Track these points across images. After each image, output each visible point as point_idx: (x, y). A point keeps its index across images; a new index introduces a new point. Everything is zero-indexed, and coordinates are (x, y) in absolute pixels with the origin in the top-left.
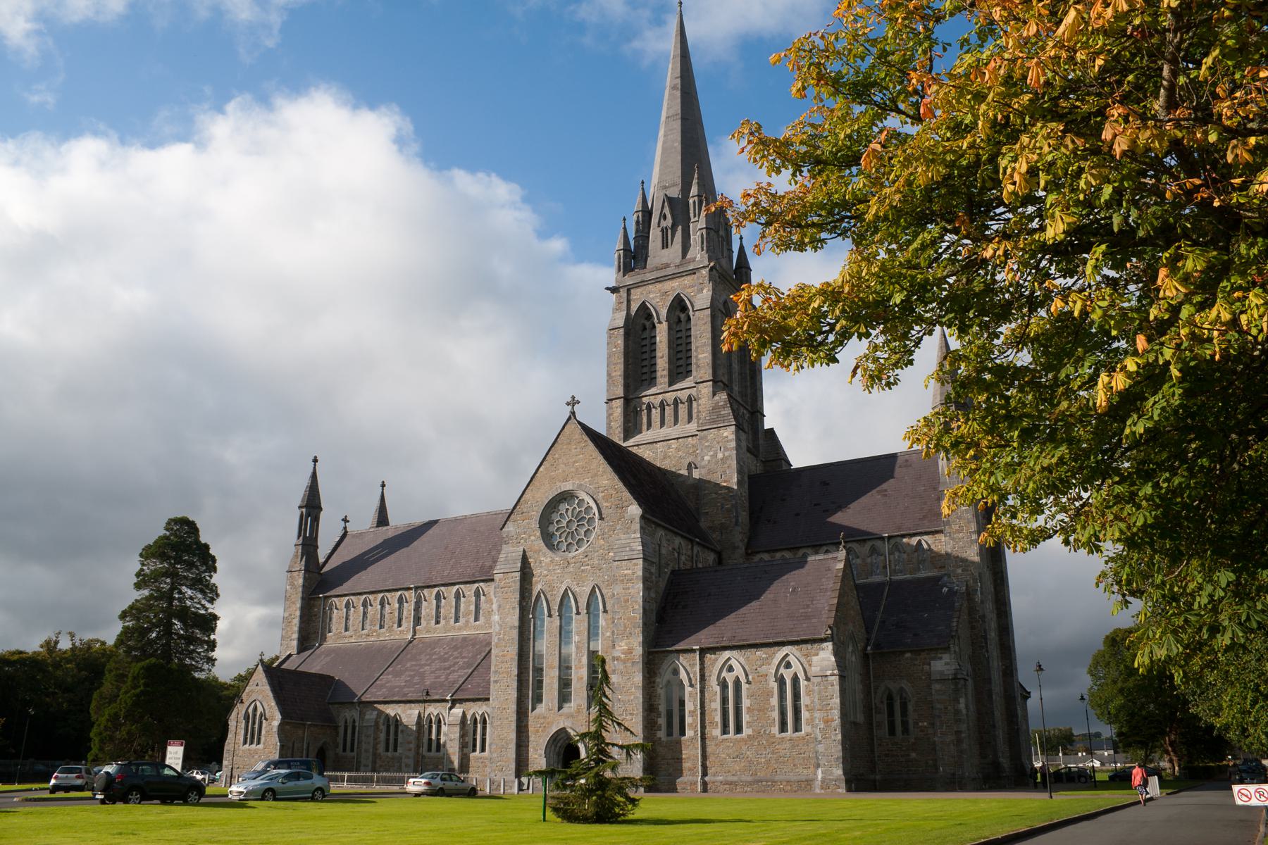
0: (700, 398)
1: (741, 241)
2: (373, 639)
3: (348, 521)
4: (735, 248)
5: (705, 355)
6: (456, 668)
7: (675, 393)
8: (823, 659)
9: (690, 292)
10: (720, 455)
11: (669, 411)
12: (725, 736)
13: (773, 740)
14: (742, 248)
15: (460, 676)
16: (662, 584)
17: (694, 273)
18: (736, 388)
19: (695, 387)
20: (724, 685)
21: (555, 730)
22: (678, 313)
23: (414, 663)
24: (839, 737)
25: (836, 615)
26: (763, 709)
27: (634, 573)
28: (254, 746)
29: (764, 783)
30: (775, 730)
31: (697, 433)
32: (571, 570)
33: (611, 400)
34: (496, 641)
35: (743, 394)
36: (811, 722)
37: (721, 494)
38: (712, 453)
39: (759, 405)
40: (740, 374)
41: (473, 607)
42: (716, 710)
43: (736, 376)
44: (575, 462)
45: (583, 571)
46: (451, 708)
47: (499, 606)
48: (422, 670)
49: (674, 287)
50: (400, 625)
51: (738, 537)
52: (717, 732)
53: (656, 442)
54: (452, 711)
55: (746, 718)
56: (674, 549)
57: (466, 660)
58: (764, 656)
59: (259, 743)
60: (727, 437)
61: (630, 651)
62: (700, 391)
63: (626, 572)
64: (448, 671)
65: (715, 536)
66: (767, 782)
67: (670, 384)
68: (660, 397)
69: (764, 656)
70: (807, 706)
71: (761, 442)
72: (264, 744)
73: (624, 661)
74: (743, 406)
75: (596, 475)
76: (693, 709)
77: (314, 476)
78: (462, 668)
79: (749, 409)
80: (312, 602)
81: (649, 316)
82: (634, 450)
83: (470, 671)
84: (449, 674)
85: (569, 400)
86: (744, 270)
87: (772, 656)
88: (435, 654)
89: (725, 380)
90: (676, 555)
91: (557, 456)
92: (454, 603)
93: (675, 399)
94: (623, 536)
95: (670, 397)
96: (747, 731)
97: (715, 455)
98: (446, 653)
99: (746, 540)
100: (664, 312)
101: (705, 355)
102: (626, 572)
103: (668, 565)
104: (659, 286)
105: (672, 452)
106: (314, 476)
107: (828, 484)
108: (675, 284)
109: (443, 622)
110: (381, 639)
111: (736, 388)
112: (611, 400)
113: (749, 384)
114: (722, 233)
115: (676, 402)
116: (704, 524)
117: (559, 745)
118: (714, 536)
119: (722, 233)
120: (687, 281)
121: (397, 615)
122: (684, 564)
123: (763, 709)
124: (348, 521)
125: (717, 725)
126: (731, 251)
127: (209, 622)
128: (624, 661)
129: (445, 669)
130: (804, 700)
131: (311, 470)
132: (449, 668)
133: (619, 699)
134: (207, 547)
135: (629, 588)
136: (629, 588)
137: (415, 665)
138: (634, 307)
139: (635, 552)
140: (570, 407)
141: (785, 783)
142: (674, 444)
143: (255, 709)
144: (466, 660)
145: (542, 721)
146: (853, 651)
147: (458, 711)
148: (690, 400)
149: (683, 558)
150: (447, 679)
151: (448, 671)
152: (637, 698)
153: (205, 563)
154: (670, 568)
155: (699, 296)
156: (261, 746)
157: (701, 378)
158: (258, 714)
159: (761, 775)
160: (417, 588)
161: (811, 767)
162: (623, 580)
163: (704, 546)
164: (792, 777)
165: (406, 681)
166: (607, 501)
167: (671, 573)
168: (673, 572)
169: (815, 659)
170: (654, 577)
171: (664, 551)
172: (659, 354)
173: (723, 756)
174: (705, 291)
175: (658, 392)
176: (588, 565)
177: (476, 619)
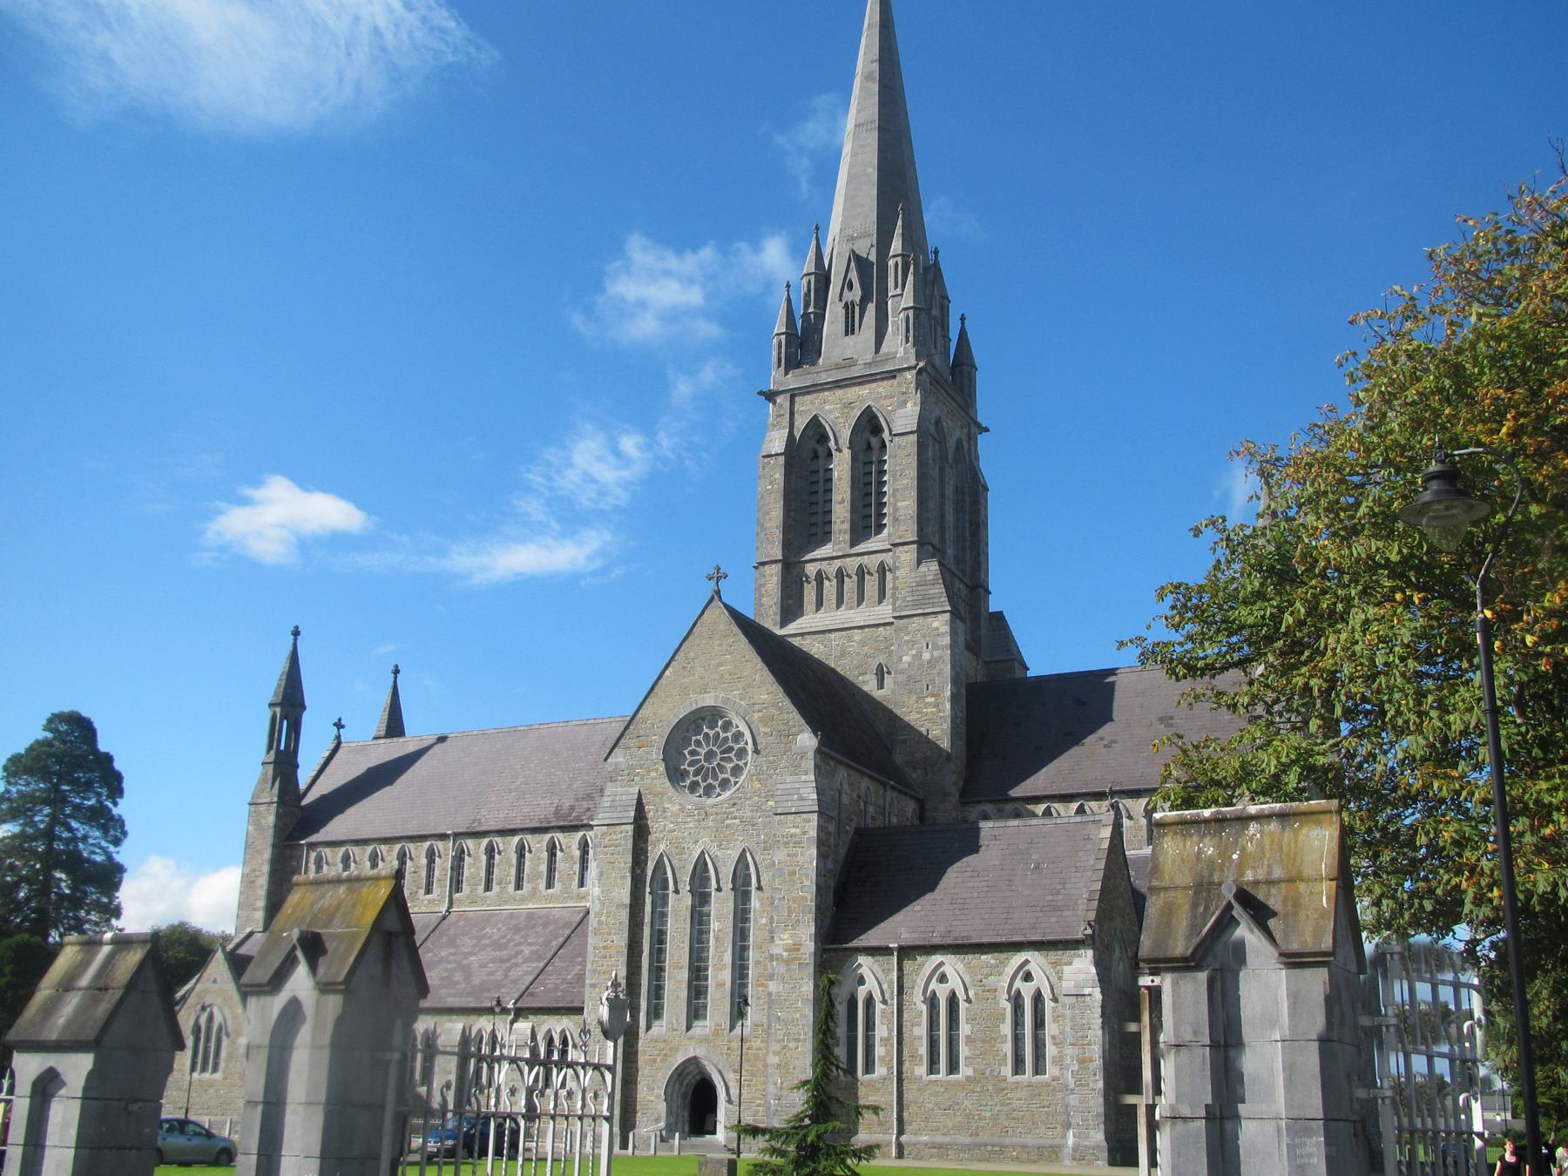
0: (898, 568)
1: (963, 323)
3: (343, 727)
4: (954, 335)
5: (906, 503)
6: (520, 959)
8: (1080, 971)
9: (882, 408)
10: (926, 656)
11: (850, 585)
12: (933, 1077)
13: (1003, 1085)
14: (963, 334)
15: (527, 973)
16: (843, 850)
17: (894, 377)
18: (950, 552)
19: (890, 550)
20: (932, 1002)
21: (680, 1059)
22: (867, 434)
23: (452, 950)
24: (1100, 1084)
25: (1099, 906)
26: (986, 1039)
27: (804, 833)
28: (207, 1075)
29: (989, 1148)
30: (1007, 1070)
31: (893, 620)
32: (711, 824)
33: (763, 564)
34: (595, 925)
35: (959, 560)
36: (1059, 1061)
37: (927, 714)
38: (914, 652)
39: (982, 576)
40: (956, 529)
41: (544, 868)
42: (920, 1038)
43: (950, 534)
44: (720, 665)
45: (728, 826)
46: (512, 1023)
47: (601, 874)
48: (464, 962)
49: (863, 395)
50: (428, 891)
51: (951, 780)
52: (921, 1070)
53: (830, 631)
54: (515, 1025)
55: (964, 1051)
56: (859, 796)
57: (535, 948)
58: (993, 961)
59: (215, 1069)
60: (937, 629)
61: (795, 948)
62: (898, 557)
63: (793, 831)
64: (508, 965)
65: (915, 776)
66: (993, 1146)
67: (854, 542)
68: (838, 563)
69: (993, 961)
70: (1053, 1037)
71: (983, 632)
73: (788, 962)
74: (961, 580)
75: (749, 686)
76: (886, 1035)
78: (527, 960)
79: (966, 581)
80: (288, 851)
81: (824, 438)
82: (796, 642)
83: (542, 965)
84: (508, 970)
85: (712, 571)
86: (966, 369)
87: (1003, 964)
88: (484, 936)
89: (935, 540)
90: (862, 804)
92: (514, 861)
93: (860, 567)
94: (789, 779)
95: (852, 564)
96: (965, 1071)
97: (919, 655)
98: (503, 937)
99: (961, 783)
100: (845, 434)
101: (906, 503)
103: (851, 821)
104: (839, 393)
105: (853, 647)
107: (1084, 704)
108: (864, 391)
109: (496, 888)
111: (950, 552)
112: (763, 564)
113: (968, 544)
114: (935, 312)
115: (861, 572)
116: (899, 757)
117: (686, 1082)
118: (915, 776)
119: (935, 312)
120: (882, 388)
121: (424, 875)
122: (873, 818)
123: (986, 1039)
124: (343, 727)
125: (921, 1059)
126: (947, 338)
127: (110, 876)
128: (788, 962)
129: (502, 961)
130: (1050, 1029)
131: (290, 648)
132: (508, 960)
133: (779, 1018)
134: (108, 759)
135: (796, 855)
136: (796, 855)
137: (455, 954)
138: (801, 423)
139: (806, 803)
140: (713, 583)
141: (1019, 1149)
142: (857, 635)
143: (211, 1018)
144: (535, 948)
145: (662, 1045)
146: (1121, 959)
147: (524, 1026)
148: (882, 570)
149: (871, 809)
150: (506, 976)
151: (508, 965)
152: (804, 1016)
153: (108, 784)
154: (854, 825)
155: (901, 412)
156: (218, 1076)
157: (900, 537)
159: (984, 1137)
160: (457, 835)
161: (1059, 1126)
162: (788, 843)
163: (900, 791)
164: (1030, 1140)
165: (442, 979)
166: (765, 726)
167: (855, 833)
168: (857, 830)
169: (1067, 969)
170: (832, 840)
171: (845, 800)
172: (836, 497)
173: (930, 1106)
174: (909, 405)
175: (834, 554)
177: (549, 885)
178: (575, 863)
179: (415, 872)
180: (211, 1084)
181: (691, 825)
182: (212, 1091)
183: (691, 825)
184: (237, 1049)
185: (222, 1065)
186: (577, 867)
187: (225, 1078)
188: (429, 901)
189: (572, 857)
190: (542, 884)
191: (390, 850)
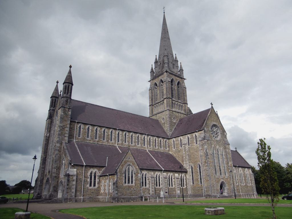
2: (100, 143)
41: (137, 141)
72: (135, 183)
77: (70, 72)
92: (131, 138)
106: (70, 72)
110: (104, 144)
121: (110, 136)
143: (129, 169)
179: (108, 136)
180: (132, 187)
182: (132, 189)
184: (138, 177)
186: (143, 142)
187: (136, 185)
188: (112, 143)
189: (142, 140)
190: (137, 144)
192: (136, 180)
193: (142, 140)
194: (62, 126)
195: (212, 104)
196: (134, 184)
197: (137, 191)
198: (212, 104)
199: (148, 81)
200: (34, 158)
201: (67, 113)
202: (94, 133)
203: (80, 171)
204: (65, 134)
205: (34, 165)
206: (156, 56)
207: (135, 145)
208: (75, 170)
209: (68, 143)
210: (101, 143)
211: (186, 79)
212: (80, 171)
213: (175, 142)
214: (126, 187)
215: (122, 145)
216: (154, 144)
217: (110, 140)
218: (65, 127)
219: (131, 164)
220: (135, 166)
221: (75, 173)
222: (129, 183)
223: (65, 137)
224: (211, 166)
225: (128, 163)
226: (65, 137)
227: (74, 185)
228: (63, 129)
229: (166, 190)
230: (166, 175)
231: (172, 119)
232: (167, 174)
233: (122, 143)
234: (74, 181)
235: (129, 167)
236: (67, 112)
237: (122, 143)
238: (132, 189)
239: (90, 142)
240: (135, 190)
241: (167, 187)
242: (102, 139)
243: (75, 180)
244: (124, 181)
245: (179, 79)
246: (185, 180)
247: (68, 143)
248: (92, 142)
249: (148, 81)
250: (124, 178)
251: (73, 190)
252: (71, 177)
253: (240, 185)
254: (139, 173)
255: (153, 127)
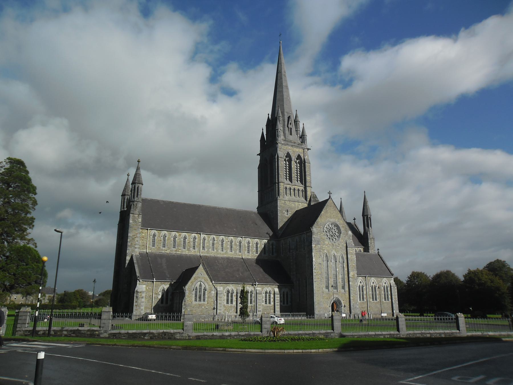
2: (179, 253)
7: (298, 187)
24: (398, 303)
27: (353, 252)
28: (202, 302)
32: (334, 247)
42: (371, 294)
44: (333, 213)
52: (371, 300)
61: (354, 275)
63: (351, 251)
69: (380, 280)
72: (207, 301)
91: (327, 209)
102: (351, 251)
121: (192, 244)
136: (352, 256)
143: (201, 285)
156: (206, 303)
158: (203, 288)
176: (339, 247)
178: (238, 246)
179: (189, 243)
180: (203, 305)
181: (331, 247)
183: (331, 247)
185: (206, 299)
186: (238, 247)
187: (208, 303)
191: (180, 235)
192: (208, 297)
193: (236, 245)
194: (131, 236)
195: (330, 193)
196: (206, 303)
197: (210, 310)
198: (330, 193)
199: (258, 155)
200: (94, 282)
201: (136, 220)
202: (171, 242)
203: (150, 288)
204: (135, 245)
205: (94, 287)
206: (268, 114)
207: (226, 252)
208: (144, 286)
209: (139, 255)
210: (180, 252)
211: (310, 149)
212: (150, 288)
213: (283, 245)
214: (195, 305)
215: (207, 254)
216: (255, 249)
217: (192, 249)
218: (135, 236)
219: (203, 280)
220: (207, 283)
221: (144, 289)
222: (200, 300)
223: (135, 248)
224: (319, 279)
225: (199, 280)
226: (135, 248)
227: (143, 302)
228: (132, 240)
229: (260, 308)
230: (261, 290)
231: (284, 213)
232: (262, 289)
233: (208, 250)
234: (143, 298)
235: (201, 283)
236: (137, 219)
237: (208, 250)
238: (202, 307)
239: (166, 252)
240: (207, 309)
241: (260, 305)
242: (182, 248)
243: (144, 297)
244: (194, 299)
245: (299, 151)
246: (289, 297)
247: (139, 255)
248: (169, 251)
249: (258, 155)
250: (194, 296)
251: (142, 307)
252: (139, 294)
253: (370, 302)
254: (212, 291)
255: (256, 224)
